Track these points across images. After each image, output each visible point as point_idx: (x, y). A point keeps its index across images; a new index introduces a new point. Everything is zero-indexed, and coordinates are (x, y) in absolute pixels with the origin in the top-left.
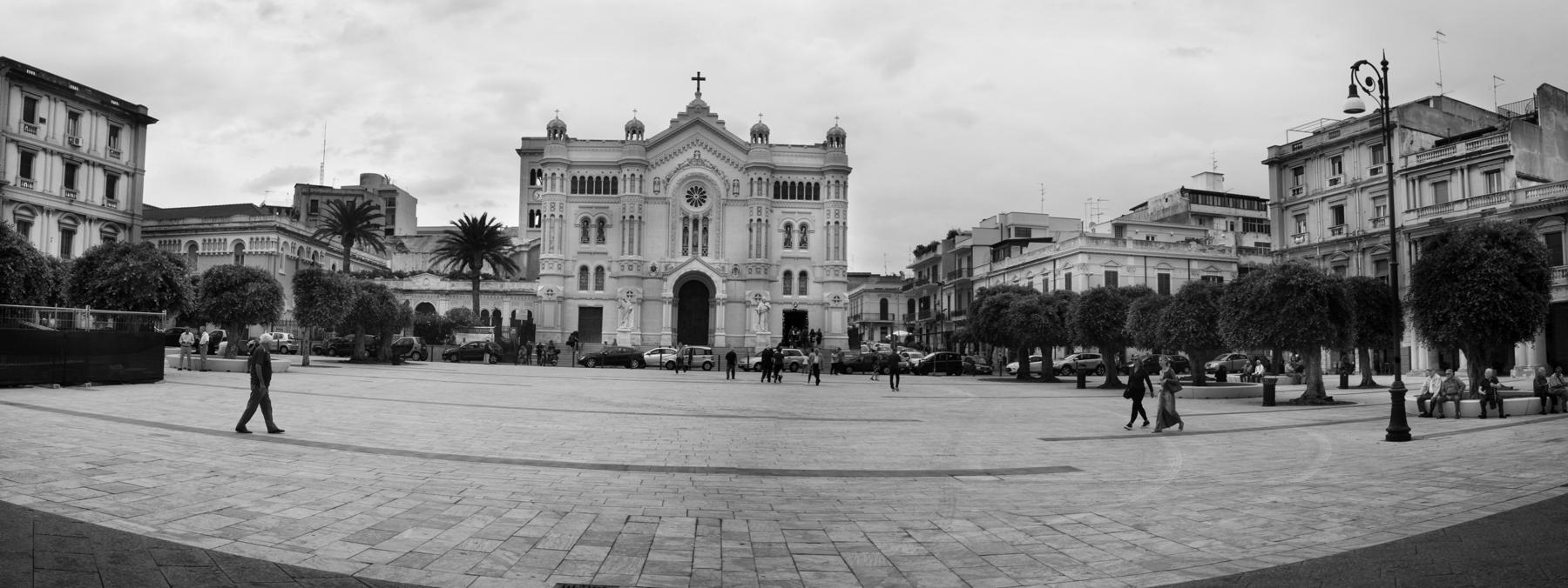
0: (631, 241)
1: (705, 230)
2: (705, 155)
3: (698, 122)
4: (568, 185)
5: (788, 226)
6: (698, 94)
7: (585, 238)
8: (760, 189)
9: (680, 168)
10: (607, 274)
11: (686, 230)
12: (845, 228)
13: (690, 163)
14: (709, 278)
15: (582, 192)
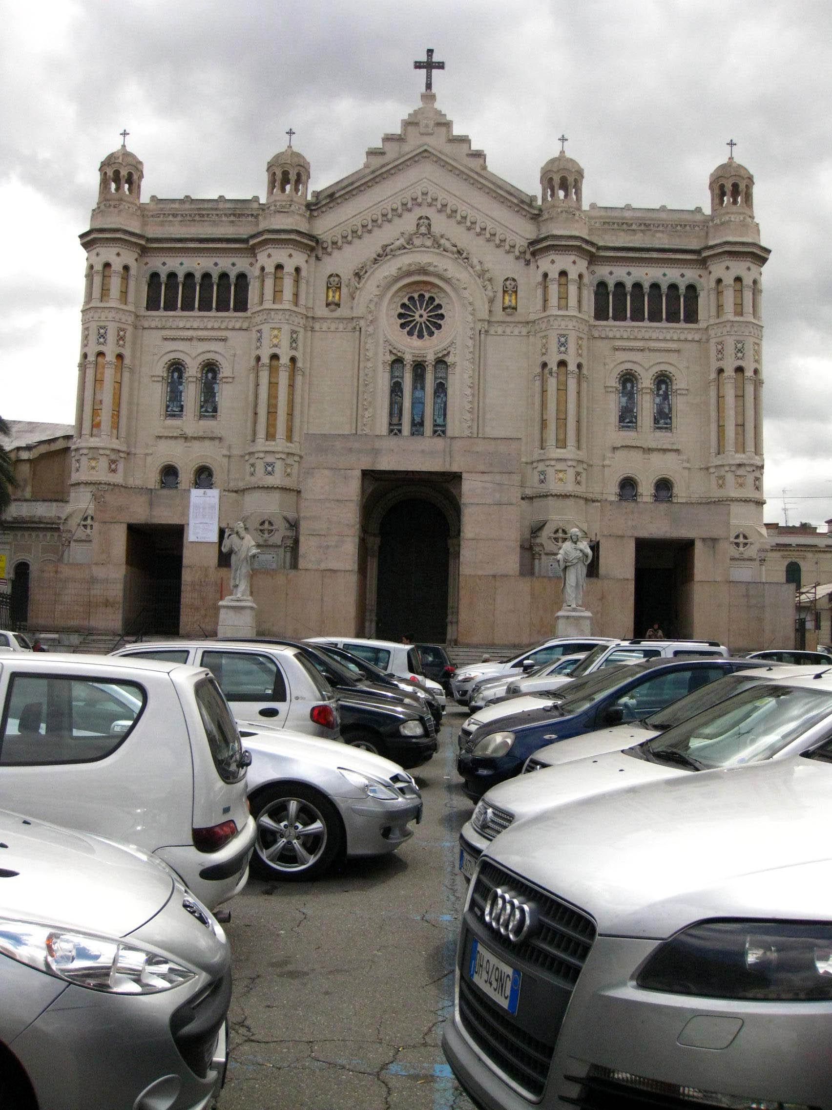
0: (272, 412)
1: (441, 389)
3: (425, 154)
4: (139, 291)
5: (628, 379)
6: (429, 96)
7: (174, 406)
8: (563, 297)
11: (396, 389)
12: (758, 383)
13: (408, 245)
15: (170, 306)
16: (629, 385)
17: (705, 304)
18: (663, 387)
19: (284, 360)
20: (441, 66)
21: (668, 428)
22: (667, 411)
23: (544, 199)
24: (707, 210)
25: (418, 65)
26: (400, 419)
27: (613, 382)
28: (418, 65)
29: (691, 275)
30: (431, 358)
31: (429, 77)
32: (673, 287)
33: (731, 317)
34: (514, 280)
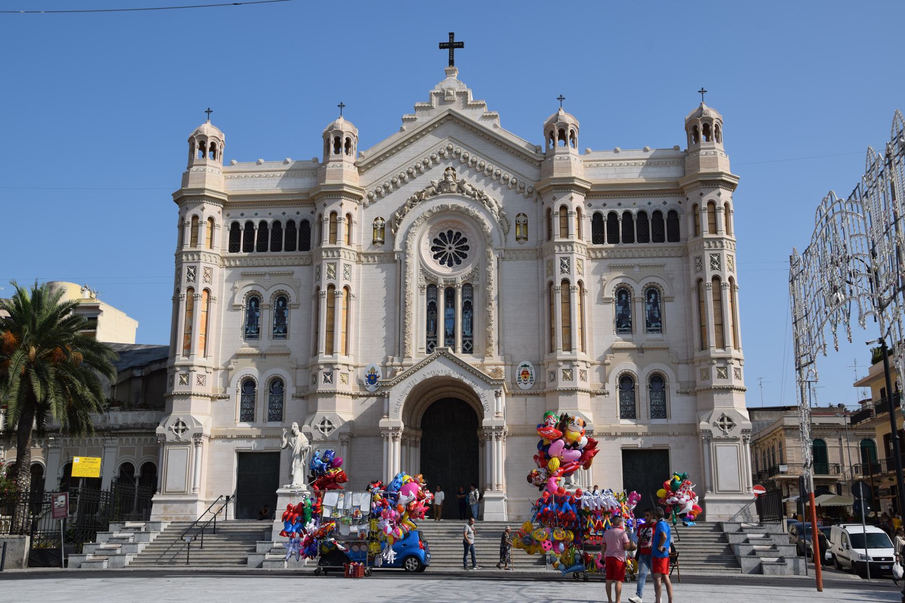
2: (462, 175)
4: (222, 236)
9: (419, 199)
10: (290, 390)
11: (432, 308)
14: (469, 389)
16: (624, 296)
17: (686, 226)
18: (653, 296)
19: (340, 289)
20: (461, 45)
21: (659, 330)
22: (657, 315)
23: (547, 147)
24: (684, 147)
25: (442, 46)
26: (435, 333)
27: (610, 293)
28: (442, 46)
29: (672, 202)
30: (460, 281)
31: (451, 55)
32: (658, 213)
33: (707, 235)
34: (524, 215)
